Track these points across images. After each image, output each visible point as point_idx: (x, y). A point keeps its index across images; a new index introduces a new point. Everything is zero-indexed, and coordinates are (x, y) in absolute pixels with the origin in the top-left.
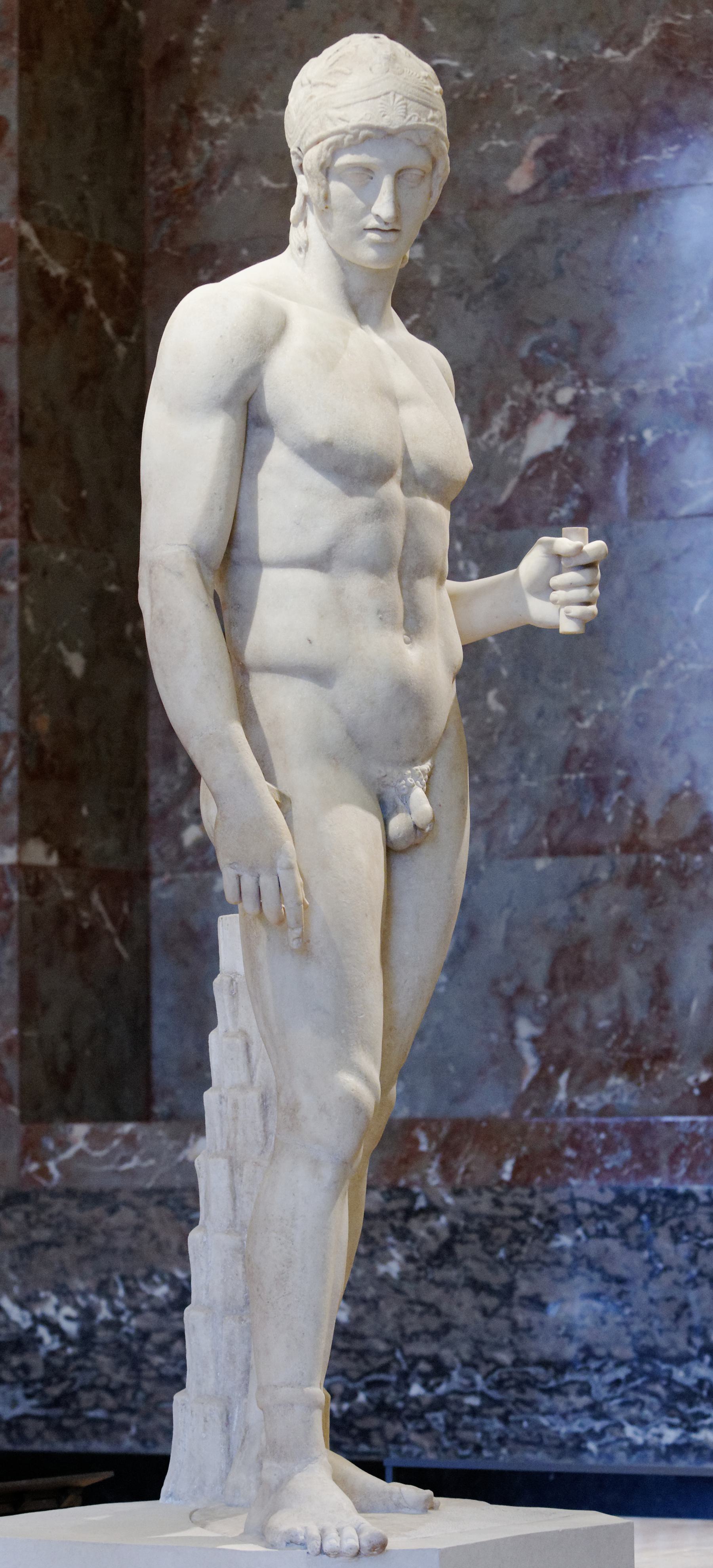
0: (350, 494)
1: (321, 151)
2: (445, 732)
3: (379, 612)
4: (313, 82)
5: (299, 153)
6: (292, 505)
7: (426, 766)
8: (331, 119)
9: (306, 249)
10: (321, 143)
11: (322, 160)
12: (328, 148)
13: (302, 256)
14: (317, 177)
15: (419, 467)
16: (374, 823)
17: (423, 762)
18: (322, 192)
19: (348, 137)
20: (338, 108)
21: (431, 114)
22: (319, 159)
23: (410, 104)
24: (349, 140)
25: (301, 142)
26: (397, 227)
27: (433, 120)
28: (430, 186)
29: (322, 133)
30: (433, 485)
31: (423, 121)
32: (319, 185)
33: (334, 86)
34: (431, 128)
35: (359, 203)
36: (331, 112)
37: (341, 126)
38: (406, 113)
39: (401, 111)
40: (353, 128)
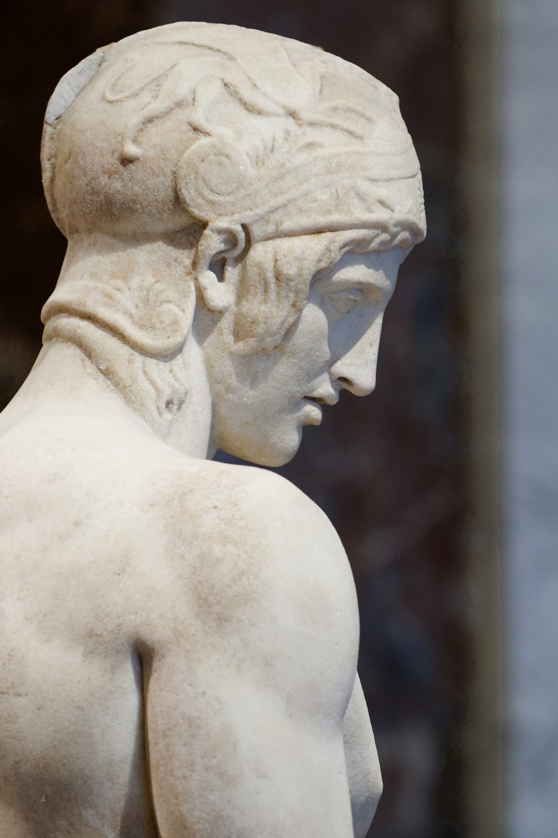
1: (328, 250)
4: (306, 115)
5: (242, 236)
8: (362, 197)
9: (181, 403)
10: (329, 235)
11: (323, 265)
12: (345, 245)
13: (168, 416)
14: (297, 292)
18: (291, 320)
19: (385, 237)
20: (374, 180)
22: (319, 261)
24: (383, 243)
25: (263, 218)
29: (336, 218)
32: (294, 305)
33: (360, 138)
35: (326, 351)
36: (365, 186)
37: (380, 215)
40: (399, 224)
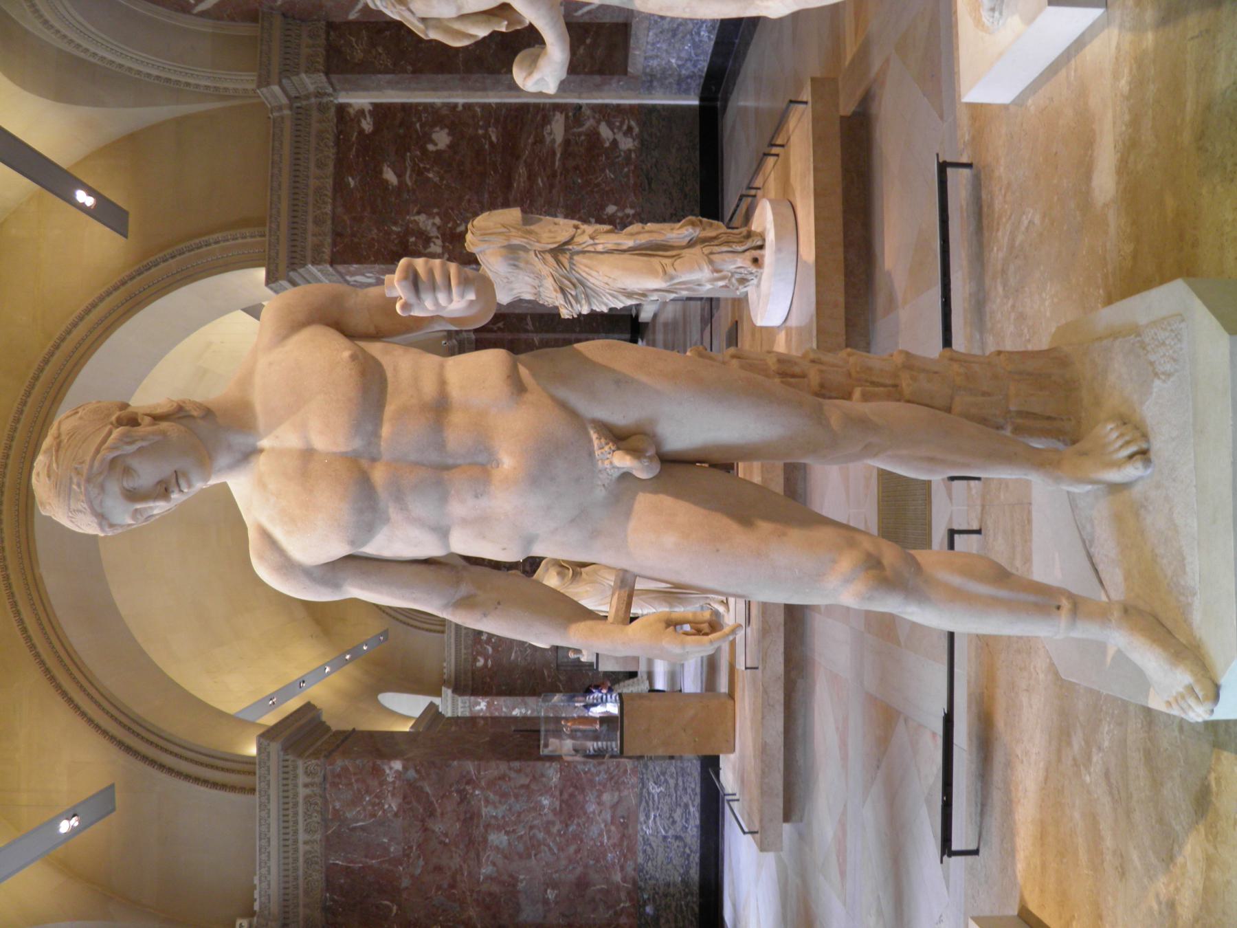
0: (388, 520)
2: (564, 406)
3: (476, 497)
6: (401, 540)
7: (594, 436)
15: (357, 444)
16: (644, 501)
17: (590, 441)
21: (74, 487)
23: (73, 506)
26: (174, 481)
27: (79, 486)
28: (134, 454)
30: (370, 427)
31: (82, 497)
34: (86, 489)
38: (80, 511)
39: (81, 516)
